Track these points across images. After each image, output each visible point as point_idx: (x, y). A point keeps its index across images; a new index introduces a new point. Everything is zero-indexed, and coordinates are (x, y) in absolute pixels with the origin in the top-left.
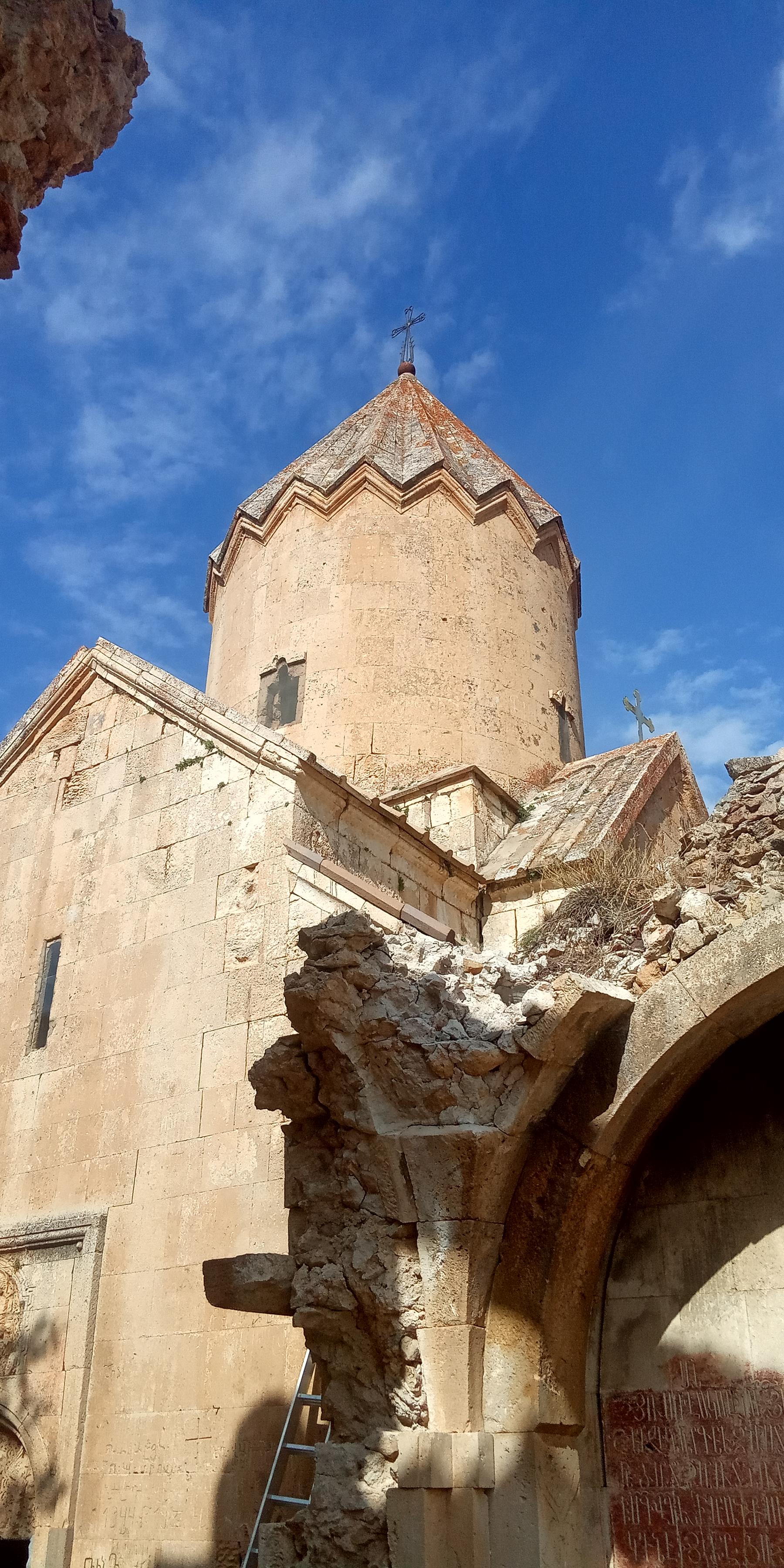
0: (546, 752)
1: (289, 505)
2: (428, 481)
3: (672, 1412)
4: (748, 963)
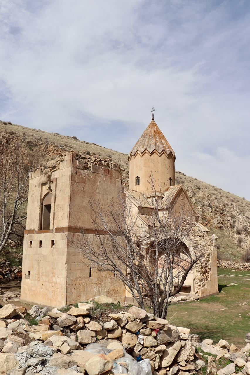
2: (153, 152)
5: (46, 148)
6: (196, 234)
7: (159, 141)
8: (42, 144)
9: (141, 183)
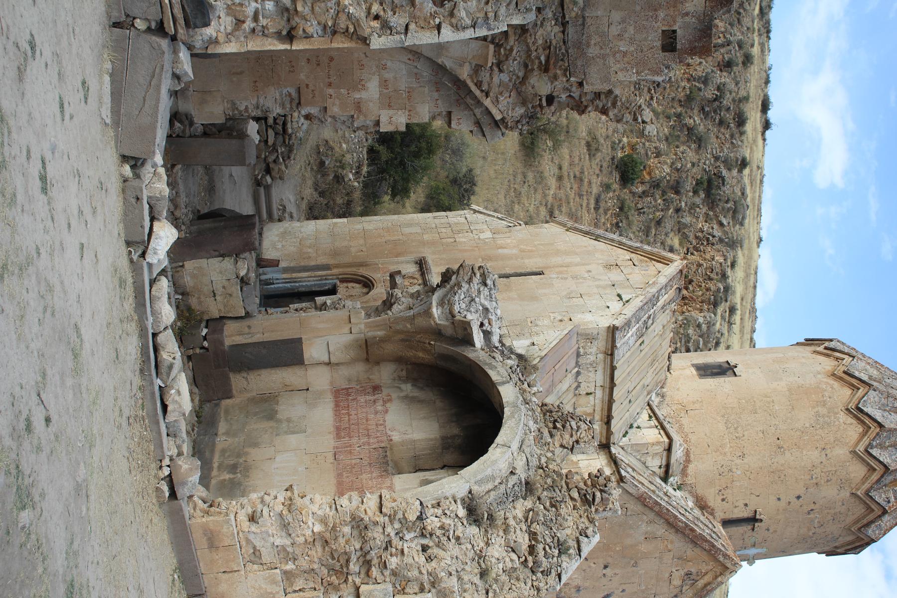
0: (723, 511)
1: (837, 359)
3: (377, 396)
4: (487, 364)
5: (711, 238)
6: (536, 527)
8: (721, 224)
9: (711, 383)
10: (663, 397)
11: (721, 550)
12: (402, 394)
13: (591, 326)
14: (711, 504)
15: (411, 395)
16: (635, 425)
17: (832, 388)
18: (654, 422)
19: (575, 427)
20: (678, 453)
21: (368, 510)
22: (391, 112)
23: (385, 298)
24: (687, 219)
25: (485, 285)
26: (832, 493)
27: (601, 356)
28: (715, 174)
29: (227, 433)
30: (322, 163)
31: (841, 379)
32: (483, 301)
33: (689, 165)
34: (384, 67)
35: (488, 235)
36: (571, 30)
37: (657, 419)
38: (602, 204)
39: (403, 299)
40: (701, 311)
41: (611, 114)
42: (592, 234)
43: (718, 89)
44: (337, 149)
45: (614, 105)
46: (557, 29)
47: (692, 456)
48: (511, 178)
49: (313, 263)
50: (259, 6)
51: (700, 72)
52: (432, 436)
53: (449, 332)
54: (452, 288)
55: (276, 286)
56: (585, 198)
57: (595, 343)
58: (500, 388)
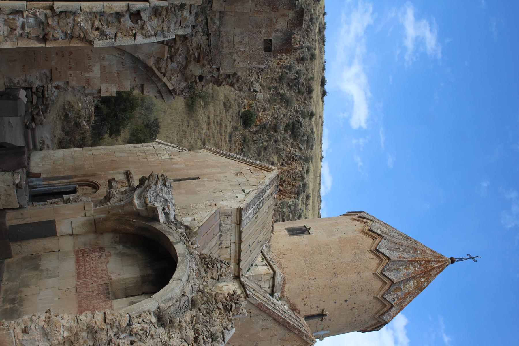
0: (305, 311)
1: (365, 222)
4: (167, 232)
5: (295, 157)
6: (198, 326)
7: (409, 271)
8: (300, 149)
10: (269, 247)
11: (304, 333)
12: (117, 252)
13: (227, 208)
14: (298, 307)
15: (122, 252)
16: (254, 264)
17: (362, 239)
18: (265, 262)
19: (219, 267)
20: (279, 279)
21: (97, 321)
22: (108, 85)
23: (106, 194)
24: (281, 146)
25: (165, 186)
26: (364, 298)
27: (233, 225)
28: (296, 121)
29: (8, 280)
30: (67, 115)
31: (367, 233)
32: (164, 195)
33: (282, 116)
34: (103, 59)
35: (167, 156)
36: (212, 38)
37: (267, 260)
38: (233, 138)
39: (117, 195)
40: (290, 198)
41: (236, 86)
42: (227, 155)
43: (297, 73)
44: (76, 107)
45: (238, 81)
46: (204, 38)
47: (287, 281)
48: (181, 123)
49: (62, 175)
50: (25, 21)
51: (286, 63)
52: (136, 276)
53: (144, 214)
54: (146, 188)
55: (39, 189)
56: (223, 135)
57: (230, 218)
58: (175, 246)
